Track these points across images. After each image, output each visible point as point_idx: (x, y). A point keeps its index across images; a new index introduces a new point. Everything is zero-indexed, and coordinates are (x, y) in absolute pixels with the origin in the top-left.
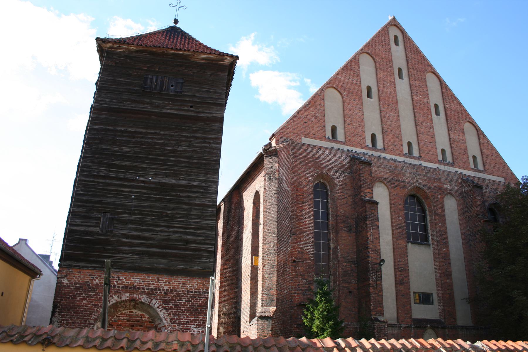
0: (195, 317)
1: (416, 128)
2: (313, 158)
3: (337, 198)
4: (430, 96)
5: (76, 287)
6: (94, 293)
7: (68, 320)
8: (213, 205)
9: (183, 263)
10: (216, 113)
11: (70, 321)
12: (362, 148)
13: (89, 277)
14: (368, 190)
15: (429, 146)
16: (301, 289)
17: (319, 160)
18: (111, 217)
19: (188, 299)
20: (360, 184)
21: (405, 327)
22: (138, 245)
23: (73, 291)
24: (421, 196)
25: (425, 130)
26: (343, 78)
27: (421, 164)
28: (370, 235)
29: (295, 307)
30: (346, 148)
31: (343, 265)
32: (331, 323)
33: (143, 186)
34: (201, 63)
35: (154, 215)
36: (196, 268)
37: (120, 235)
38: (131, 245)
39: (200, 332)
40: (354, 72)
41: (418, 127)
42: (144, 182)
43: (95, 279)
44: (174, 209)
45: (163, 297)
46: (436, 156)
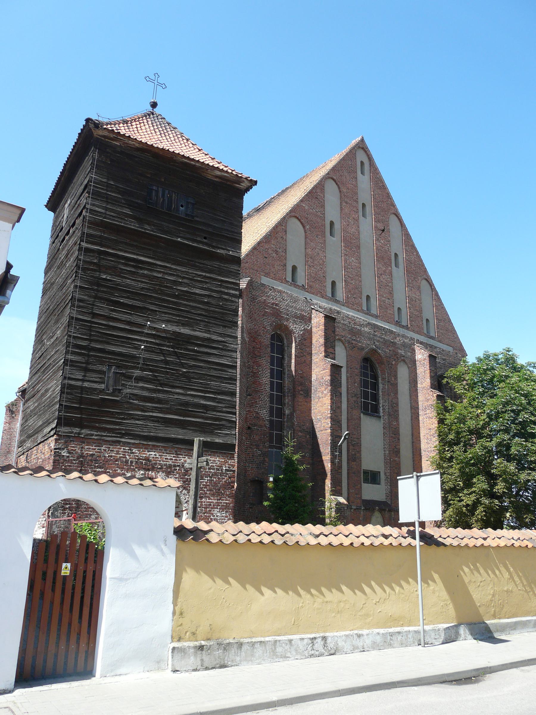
13: (95, 449)
24: (376, 360)
26: (307, 206)
34: (214, 181)
39: (223, 516)
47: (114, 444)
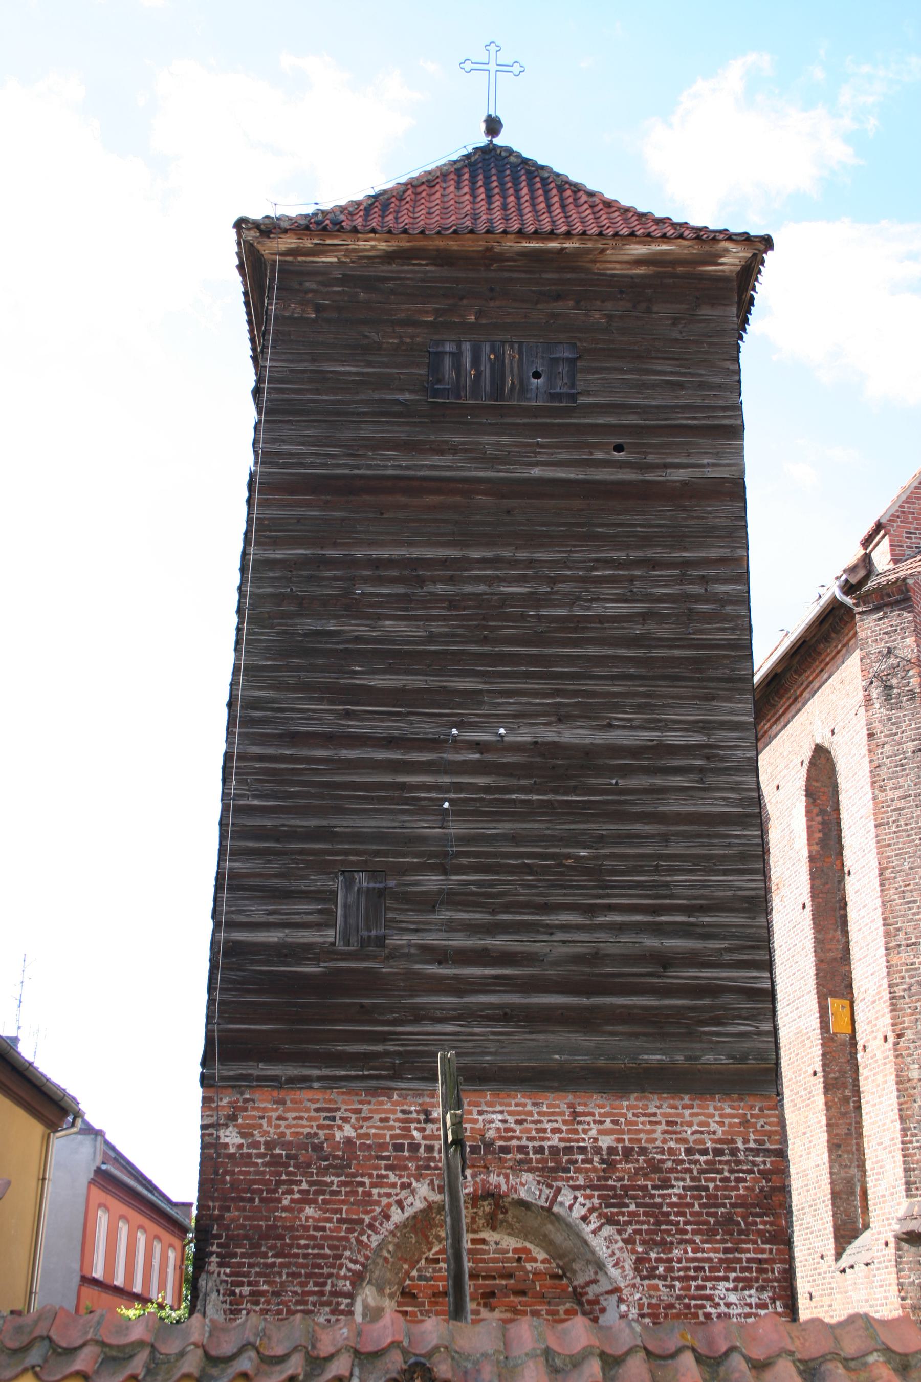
0: (726, 1251)
5: (272, 1156)
6: (343, 1178)
7: (257, 1283)
9: (658, 1045)
10: (714, 465)
11: (265, 1287)
18: (372, 885)
23: (263, 1173)
33: (478, 761)
34: (631, 277)
35: (529, 870)
36: (709, 1058)
37: (413, 951)
38: (459, 987)
39: (750, 1306)
42: (478, 746)
43: (340, 1122)
44: (601, 840)
45: (599, 1179)
47: (373, 1100)
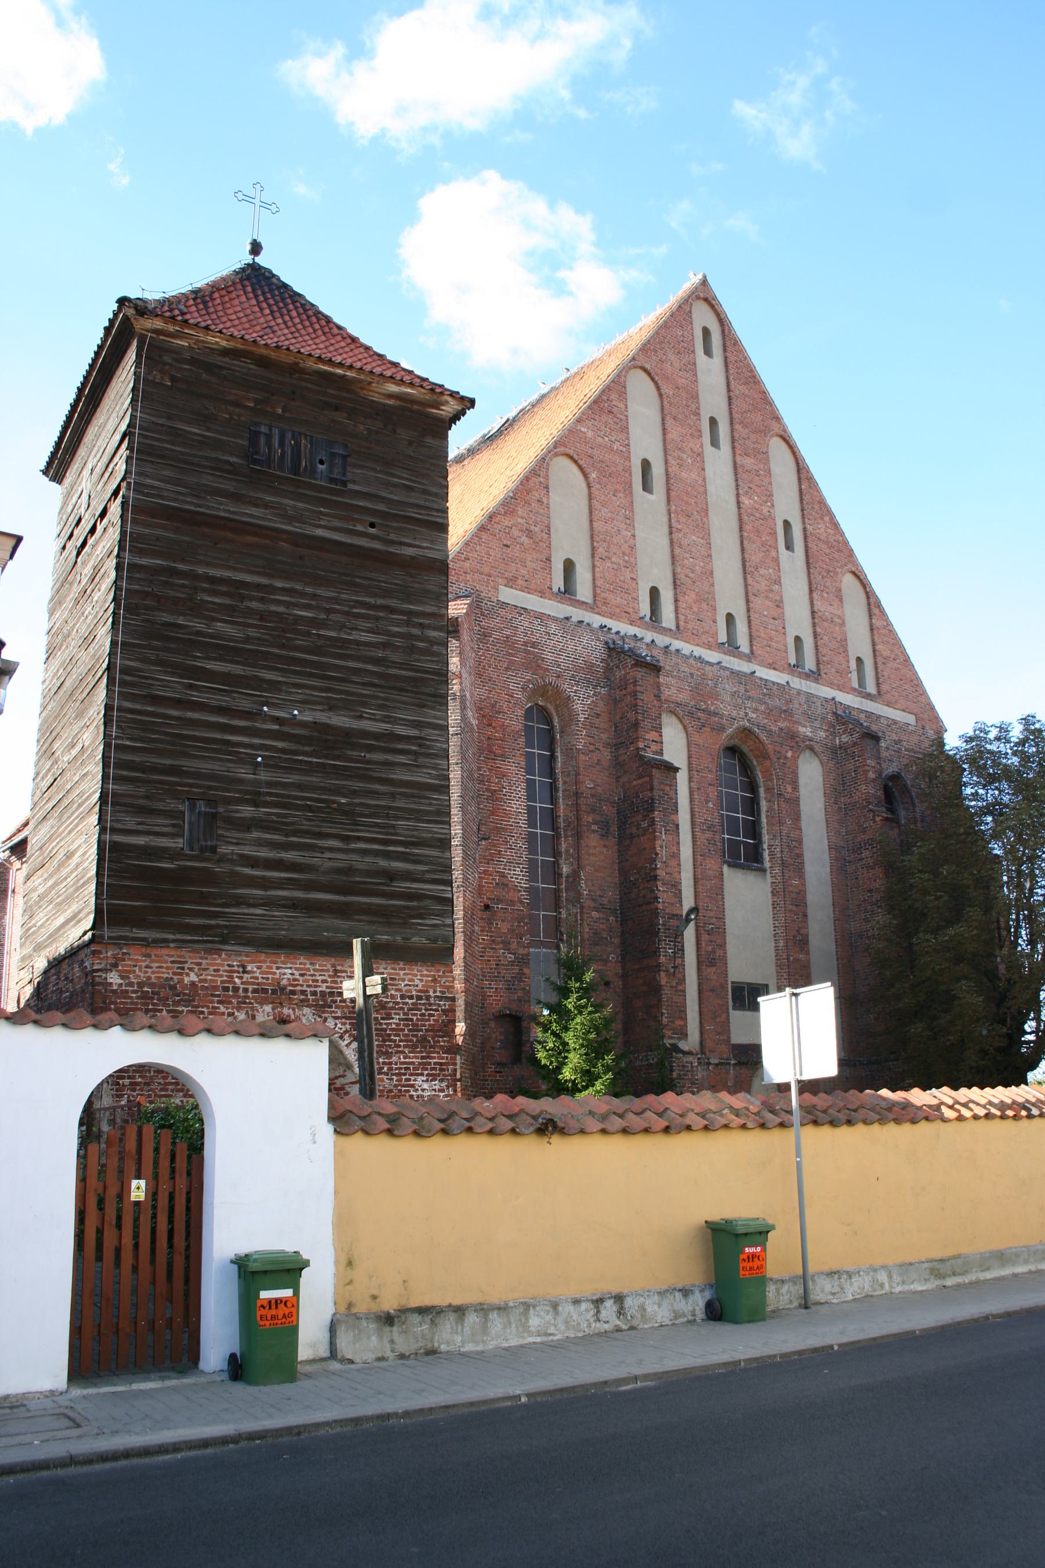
0: (422, 1058)
1: (745, 579)
2: (525, 644)
3: (579, 750)
4: (776, 498)
5: (143, 992)
6: (190, 1008)
7: (134, 1077)
8: (442, 786)
9: (386, 929)
10: (431, 549)
11: (140, 1080)
12: (632, 623)
13: (172, 968)
14: (652, 735)
15: (770, 626)
16: (503, 977)
17: (539, 649)
18: (208, 810)
19: (404, 1014)
20: (637, 719)
21: (717, 1065)
22: (280, 884)
23: (136, 1003)
24: (751, 750)
25: (763, 586)
26: (590, 432)
27: (754, 672)
28: (661, 847)
29: (491, 1020)
30: (597, 620)
31: (592, 918)
32: (609, 1059)
33: (278, 731)
34: (384, 405)
35: (310, 809)
36: (415, 939)
37: (235, 857)
38: (265, 884)
39: (435, 1090)
40: (615, 419)
41: (749, 577)
42: (277, 720)
43: (187, 971)
44: (354, 793)
45: (350, 1013)
46: (784, 655)
47: (209, 957)
